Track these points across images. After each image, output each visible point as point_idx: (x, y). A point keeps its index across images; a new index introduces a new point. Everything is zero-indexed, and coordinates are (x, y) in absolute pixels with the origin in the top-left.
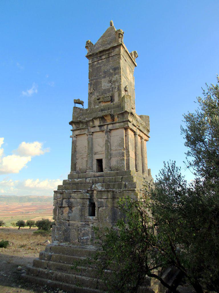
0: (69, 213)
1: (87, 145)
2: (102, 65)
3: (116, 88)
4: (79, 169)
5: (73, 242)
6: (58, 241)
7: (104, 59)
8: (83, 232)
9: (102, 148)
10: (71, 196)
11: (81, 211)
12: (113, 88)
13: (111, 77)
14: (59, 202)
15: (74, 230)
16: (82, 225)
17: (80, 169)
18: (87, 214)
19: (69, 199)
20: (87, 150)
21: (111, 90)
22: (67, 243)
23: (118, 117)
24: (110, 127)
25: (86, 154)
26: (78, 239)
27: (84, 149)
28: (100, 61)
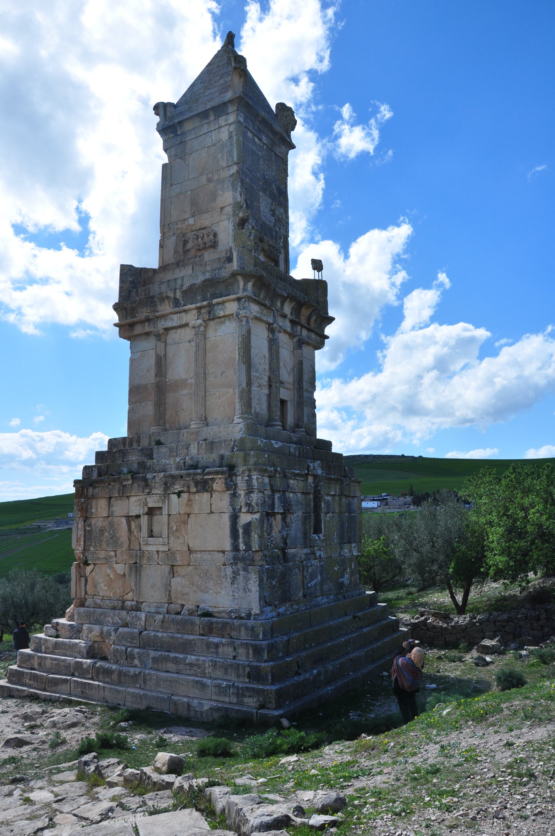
0: (283, 528)
1: (267, 355)
2: (260, 153)
3: (280, 238)
4: (255, 411)
5: (296, 599)
6: (270, 605)
7: (264, 144)
8: (310, 570)
9: (289, 374)
10: (288, 486)
11: (304, 523)
12: (276, 232)
13: (274, 203)
14: (267, 499)
15: (297, 570)
16: (306, 554)
17: (257, 414)
18: (312, 530)
19: (284, 492)
20: (267, 367)
21: (274, 233)
22: (288, 605)
23: (315, 321)
24: (305, 332)
25: (267, 379)
26: (304, 590)
27: (263, 361)
28: (256, 140)
